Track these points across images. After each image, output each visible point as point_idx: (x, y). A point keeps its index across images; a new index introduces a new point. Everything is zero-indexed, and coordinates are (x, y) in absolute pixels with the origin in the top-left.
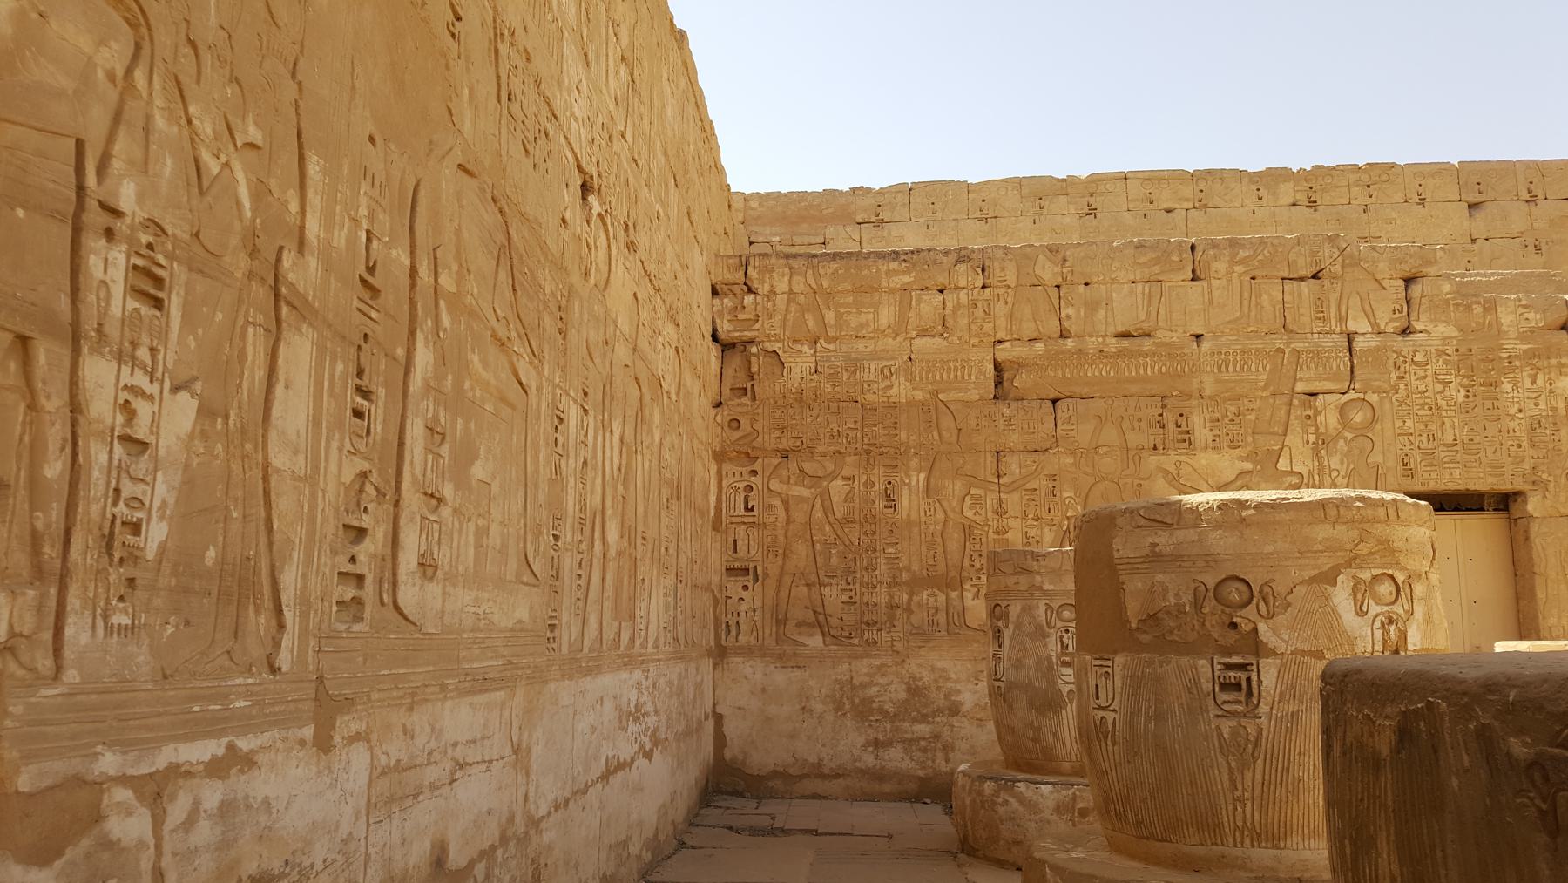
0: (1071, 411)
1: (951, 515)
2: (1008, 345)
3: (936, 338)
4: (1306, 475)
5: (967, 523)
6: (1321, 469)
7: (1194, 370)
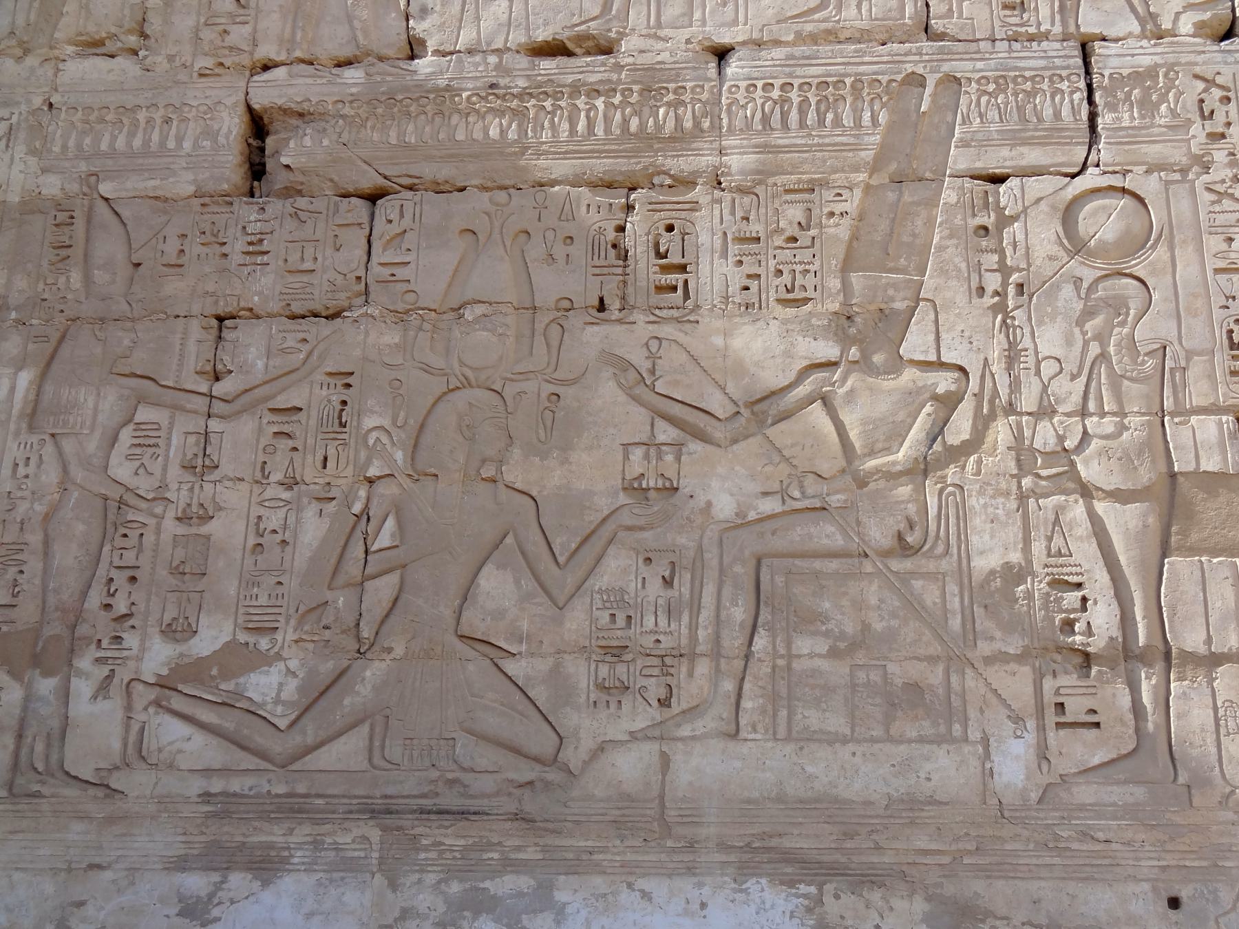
0: (407, 222)
1: (78, 474)
2: (280, 73)
3: (118, 59)
5: (114, 493)
6: (1012, 355)
7: (706, 124)
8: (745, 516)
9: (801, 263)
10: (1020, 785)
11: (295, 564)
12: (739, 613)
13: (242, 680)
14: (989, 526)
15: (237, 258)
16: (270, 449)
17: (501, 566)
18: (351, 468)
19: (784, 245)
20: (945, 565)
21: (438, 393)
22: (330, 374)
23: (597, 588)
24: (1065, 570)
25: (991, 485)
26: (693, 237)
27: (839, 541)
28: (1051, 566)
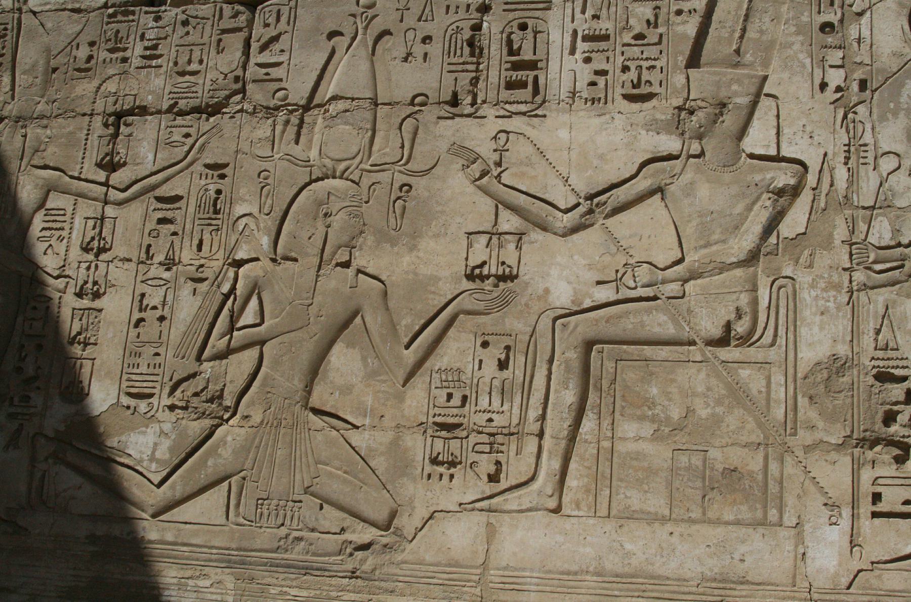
4: (814, 165)
8: (581, 304)
9: (647, 59)
10: (832, 571)
11: (171, 337)
12: (570, 397)
13: (123, 438)
14: (818, 318)
15: (136, 62)
16: (155, 234)
17: (350, 345)
18: (222, 252)
19: (633, 42)
20: (774, 354)
21: (301, 183)
22: (207, 166)
23: (437, 368)
24: (891, 363)
25: (824, 278)
26: (545, 35)
27: (670, 331)
28: (878, 359)
